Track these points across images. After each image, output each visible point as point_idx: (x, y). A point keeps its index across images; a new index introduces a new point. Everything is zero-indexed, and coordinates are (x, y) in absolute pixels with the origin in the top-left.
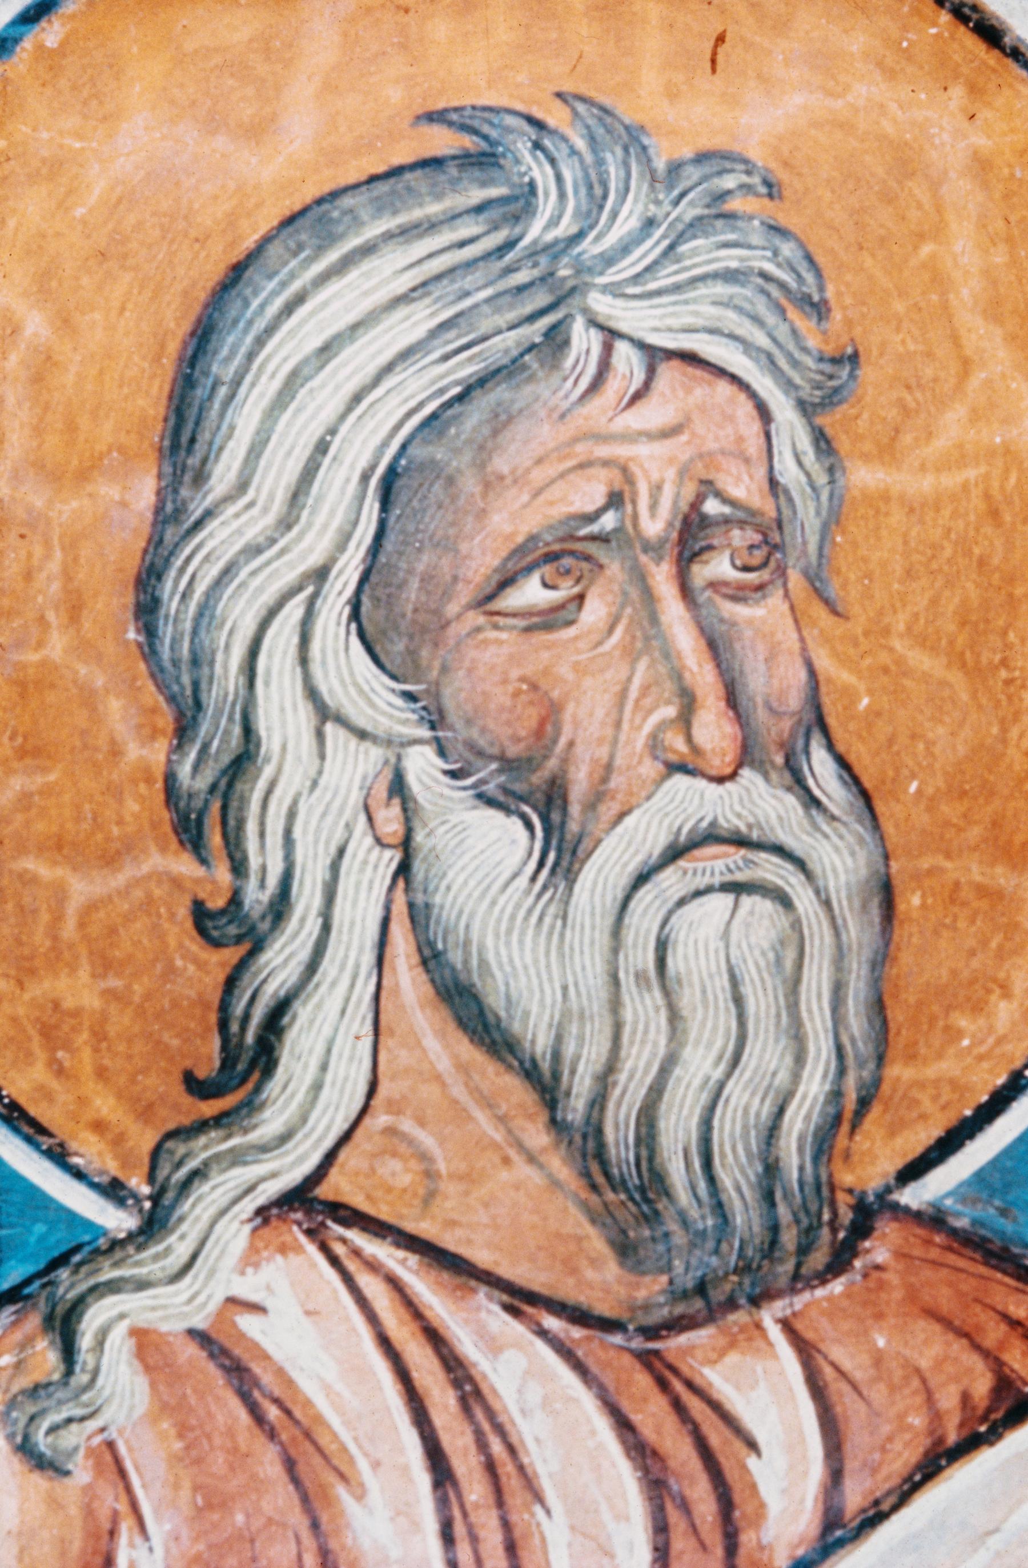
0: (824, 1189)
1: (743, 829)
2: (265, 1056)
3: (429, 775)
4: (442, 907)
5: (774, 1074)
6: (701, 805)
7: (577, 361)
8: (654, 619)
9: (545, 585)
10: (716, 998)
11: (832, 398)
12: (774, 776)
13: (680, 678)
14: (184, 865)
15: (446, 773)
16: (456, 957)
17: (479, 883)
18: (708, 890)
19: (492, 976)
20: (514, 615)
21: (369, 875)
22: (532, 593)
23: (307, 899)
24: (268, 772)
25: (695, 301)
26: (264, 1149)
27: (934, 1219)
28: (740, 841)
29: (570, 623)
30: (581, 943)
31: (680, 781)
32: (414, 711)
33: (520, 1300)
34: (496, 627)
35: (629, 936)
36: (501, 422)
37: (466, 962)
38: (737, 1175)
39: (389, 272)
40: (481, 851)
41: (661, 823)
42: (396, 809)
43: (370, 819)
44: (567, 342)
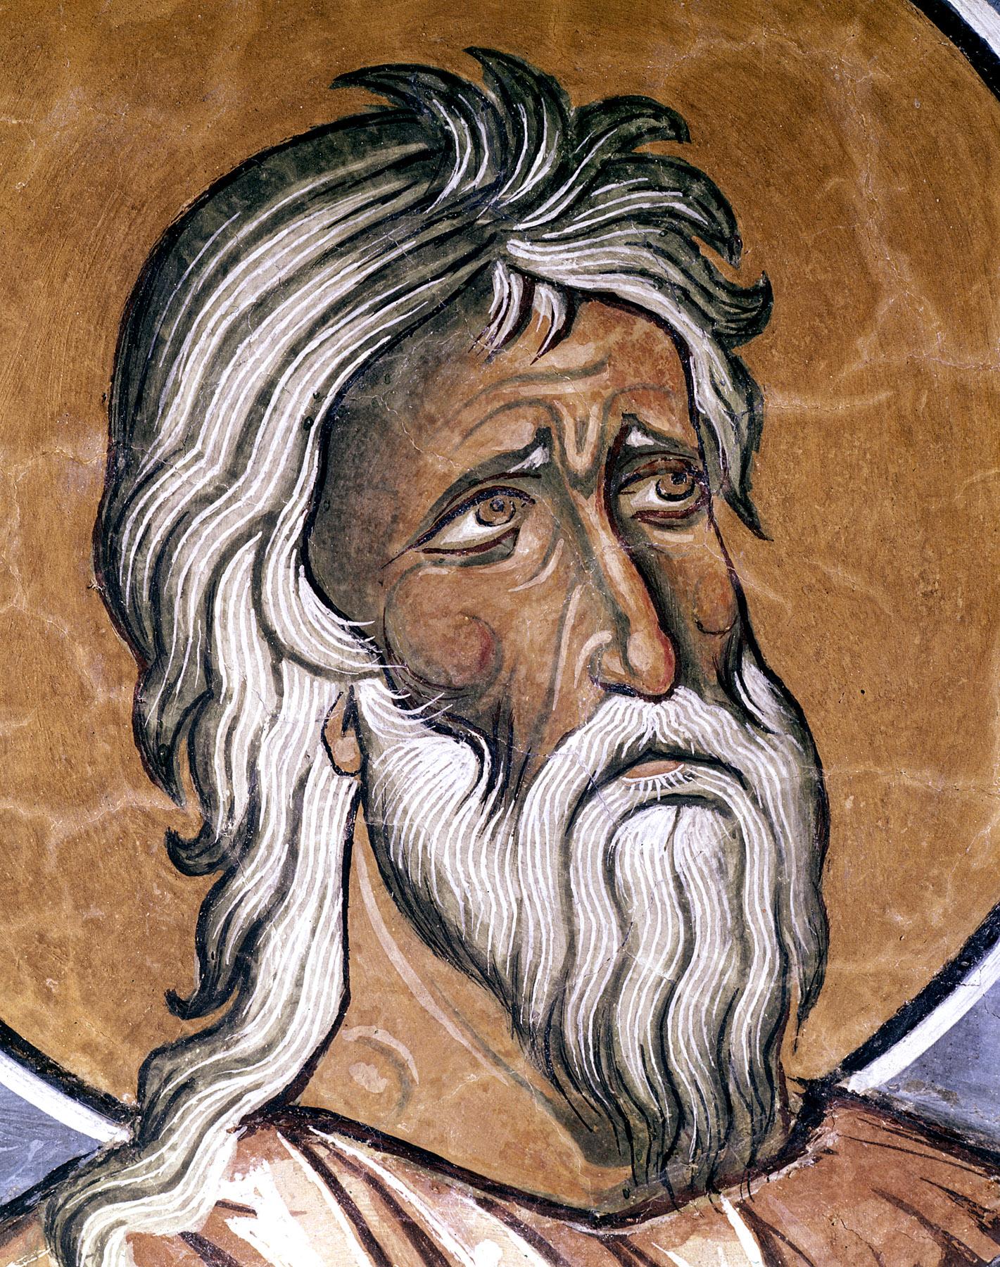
0: (769, 1074)
1: (681, 744)
2: (243, 973)
3: (381, 706)
4: (400, 830)
5: (723, 973)
6: (640, 722)
7: (500, 306)
8: (587, 550)
9: (480, 522)
10: (663, 904)
11: (753, 326)
12: (708, 693)
13: (614, 603)
14: (157, 800)
15: (395, 702)
16: (416, 876)
17: (434, 806)
18: (653, 802)
19: (452, 892)
20: (453, 552)
21: (329, 802)
22: (468, 529)
23: (274, 825)
24: (230, 709)
25: (611, 243)
26: (245, 1061)
27: (879, 1105)
28: (677, 755)
29: (509, 556)
30: (533, 858)
31: (619, 702)
32: (363, 646)
33: (492, 1193)
34: (440, 563)
35: (578, 850)
36: (429, 367)
37: (425, 880)
38: (689, 1064)
39: (315, 230)
40: (433, 774)
41: (602, 741)
42: (351, 738)
43: (328, 749)
44: (490, 289)
